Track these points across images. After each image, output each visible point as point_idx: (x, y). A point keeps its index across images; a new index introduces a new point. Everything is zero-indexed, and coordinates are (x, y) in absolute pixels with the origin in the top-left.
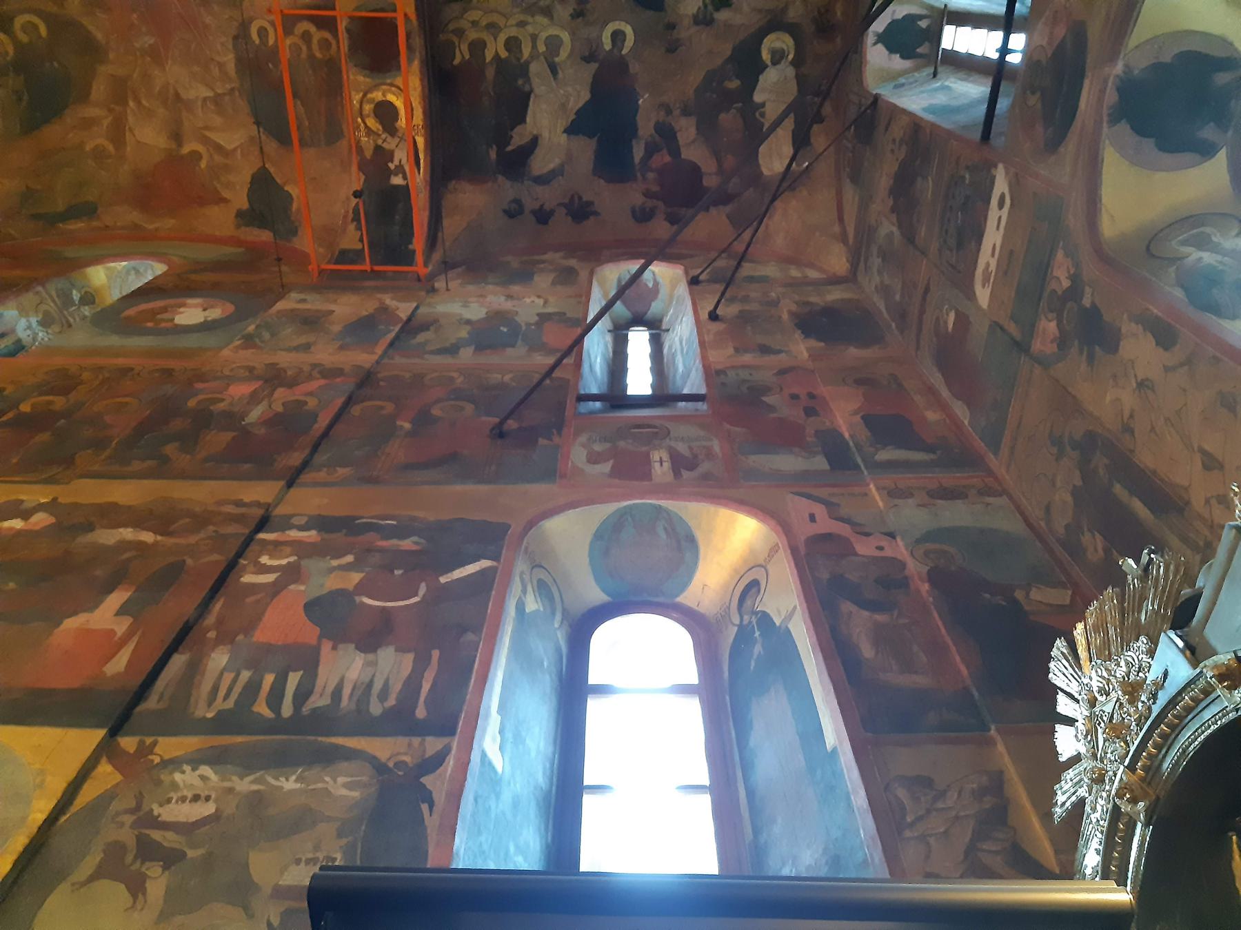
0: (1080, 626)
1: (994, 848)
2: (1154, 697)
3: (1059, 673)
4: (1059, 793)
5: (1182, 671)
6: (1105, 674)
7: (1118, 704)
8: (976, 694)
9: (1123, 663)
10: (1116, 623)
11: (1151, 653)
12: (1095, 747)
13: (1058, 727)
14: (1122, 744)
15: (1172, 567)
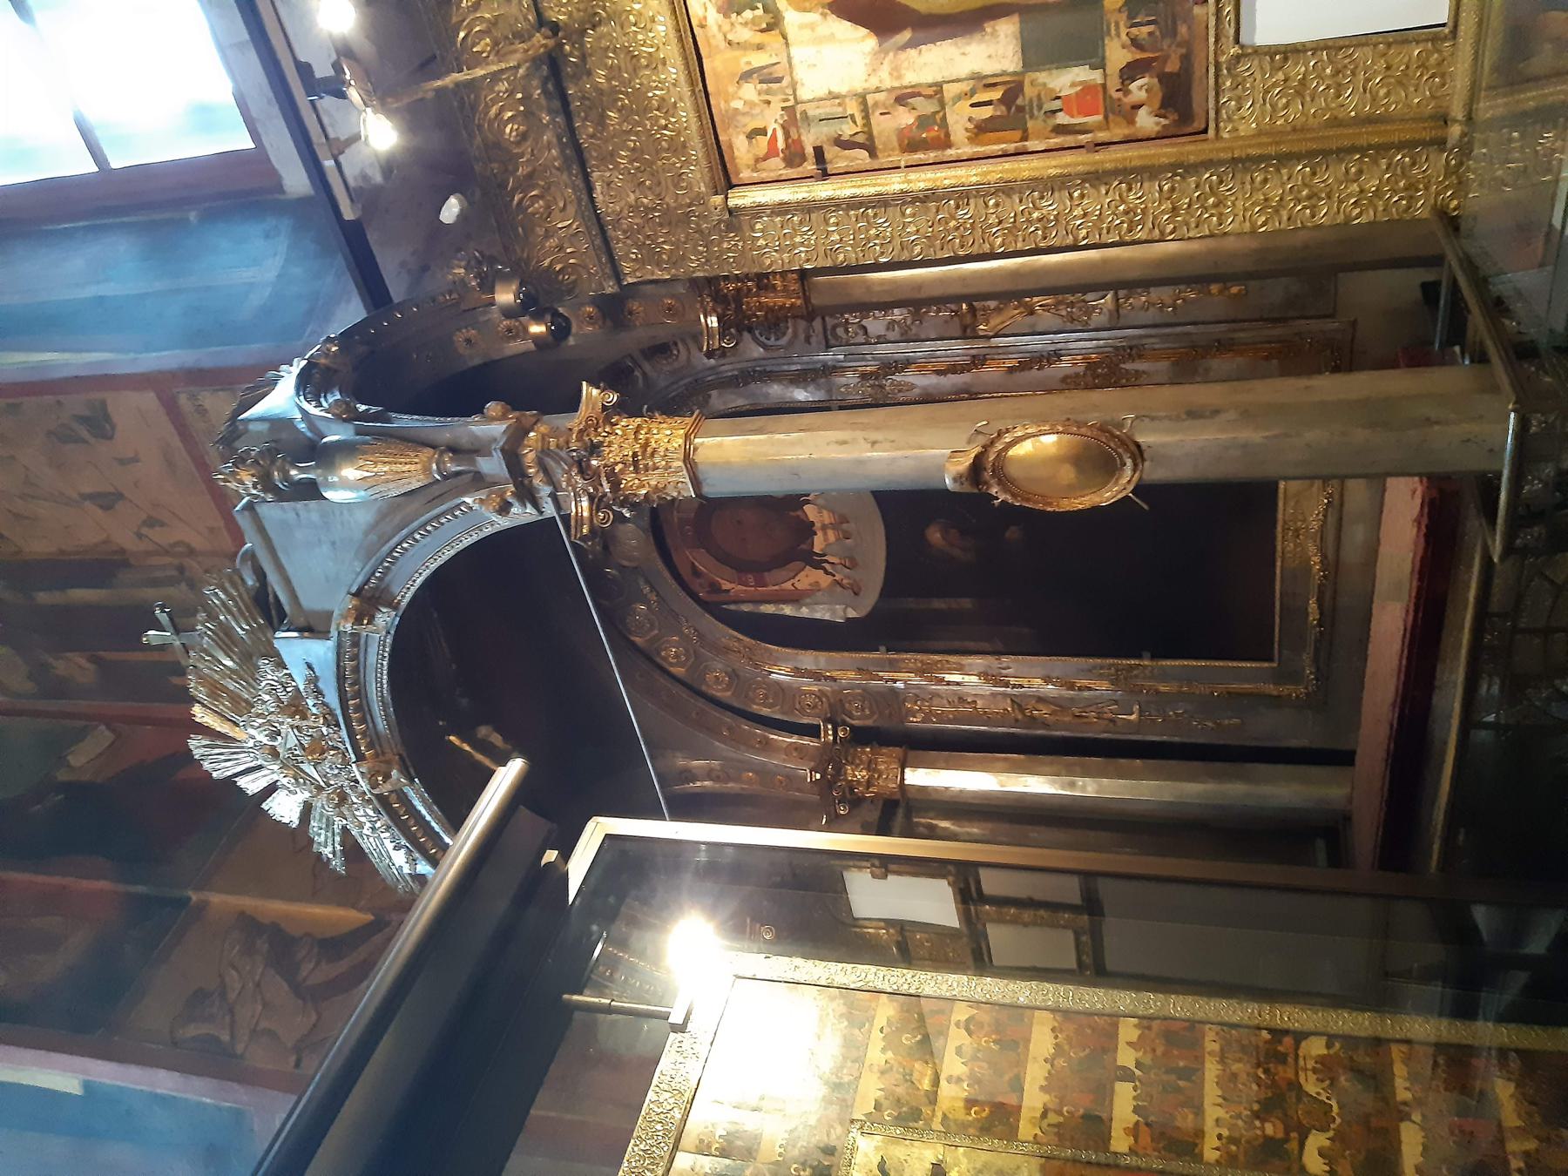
0: (197, 710)
1: (311, 966)
2: (318, 693)
3: (219, 766)
4: (322, 849)
5: (321, 651)
6: (261, 721)
7: (295, 730)
8: (140, 889)
9: (266, 697)
10: (226, 674)
11: (281, 665)
12: (313, 782)
13: (265, 806)
14: (332, 752)
15: (227, 585)
